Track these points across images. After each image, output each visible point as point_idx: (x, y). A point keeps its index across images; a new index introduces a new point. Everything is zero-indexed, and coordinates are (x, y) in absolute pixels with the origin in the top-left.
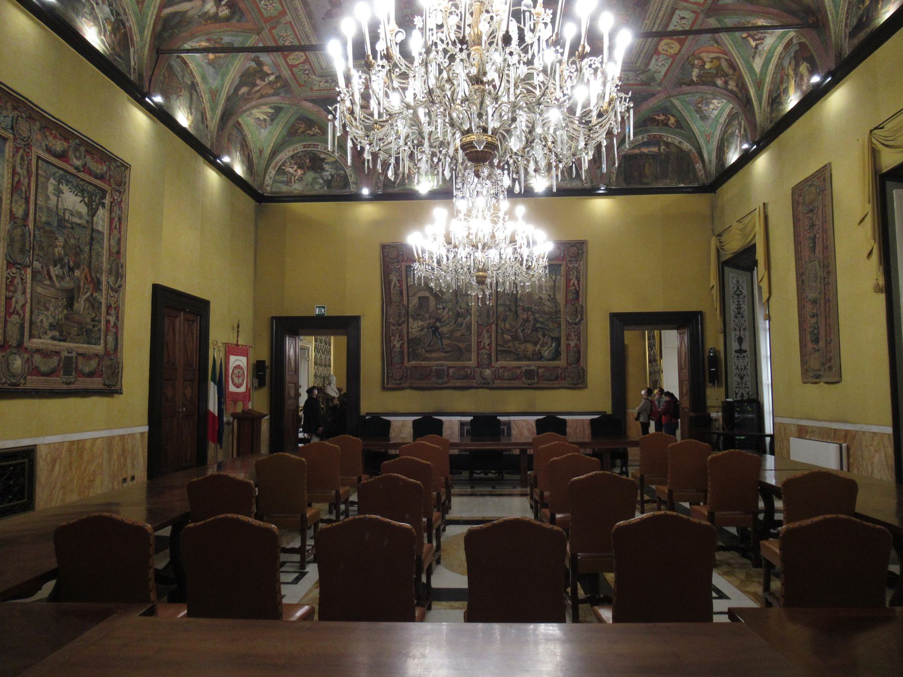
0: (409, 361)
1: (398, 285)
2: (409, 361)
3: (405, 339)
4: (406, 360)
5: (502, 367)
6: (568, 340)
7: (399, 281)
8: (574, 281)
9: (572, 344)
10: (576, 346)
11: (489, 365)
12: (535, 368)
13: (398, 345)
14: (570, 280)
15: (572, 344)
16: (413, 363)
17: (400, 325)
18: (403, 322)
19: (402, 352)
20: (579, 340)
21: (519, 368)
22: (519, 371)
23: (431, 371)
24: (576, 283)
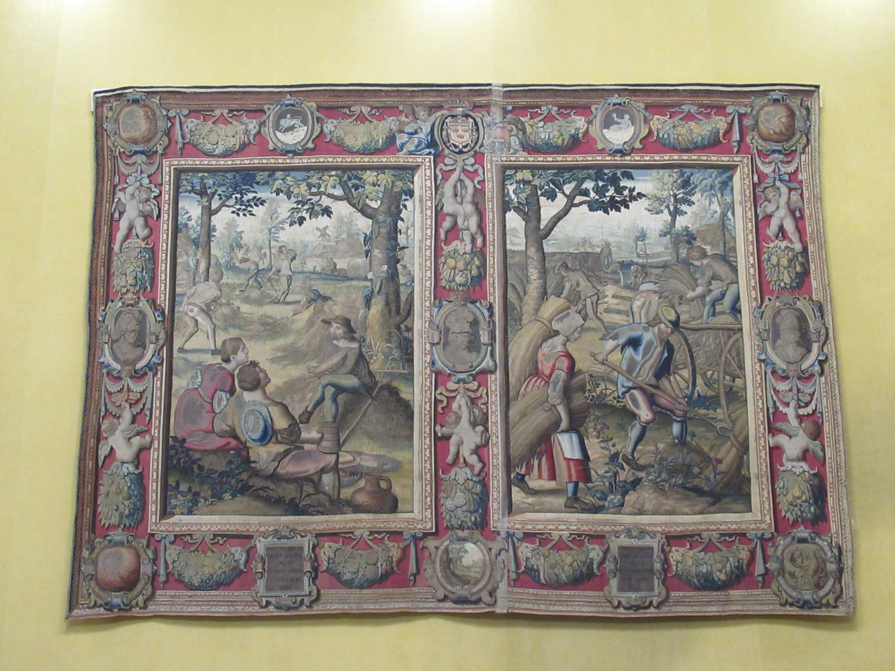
0: (165, 513)
1: (140, 229)
2: (165, 513)
3: (157, 431)
4: (153, 507)
5: (528, 536)
6: (773, 430)
7: (147, 217)
8: (781, 217)
9: (792, 446)
10: (805, 455)
11: (482, 525)
12: (654, 544)
13: (124, 452)
14: (769, 217)
15: (792, 446)
16: (182, 521)
17: (138, 376)
18: (152, 367)
19: (140, 480)
20: (817, 434)
21: (598, 538)
22: (595, 552)
23: (250, 552)
24: (789, 226)
